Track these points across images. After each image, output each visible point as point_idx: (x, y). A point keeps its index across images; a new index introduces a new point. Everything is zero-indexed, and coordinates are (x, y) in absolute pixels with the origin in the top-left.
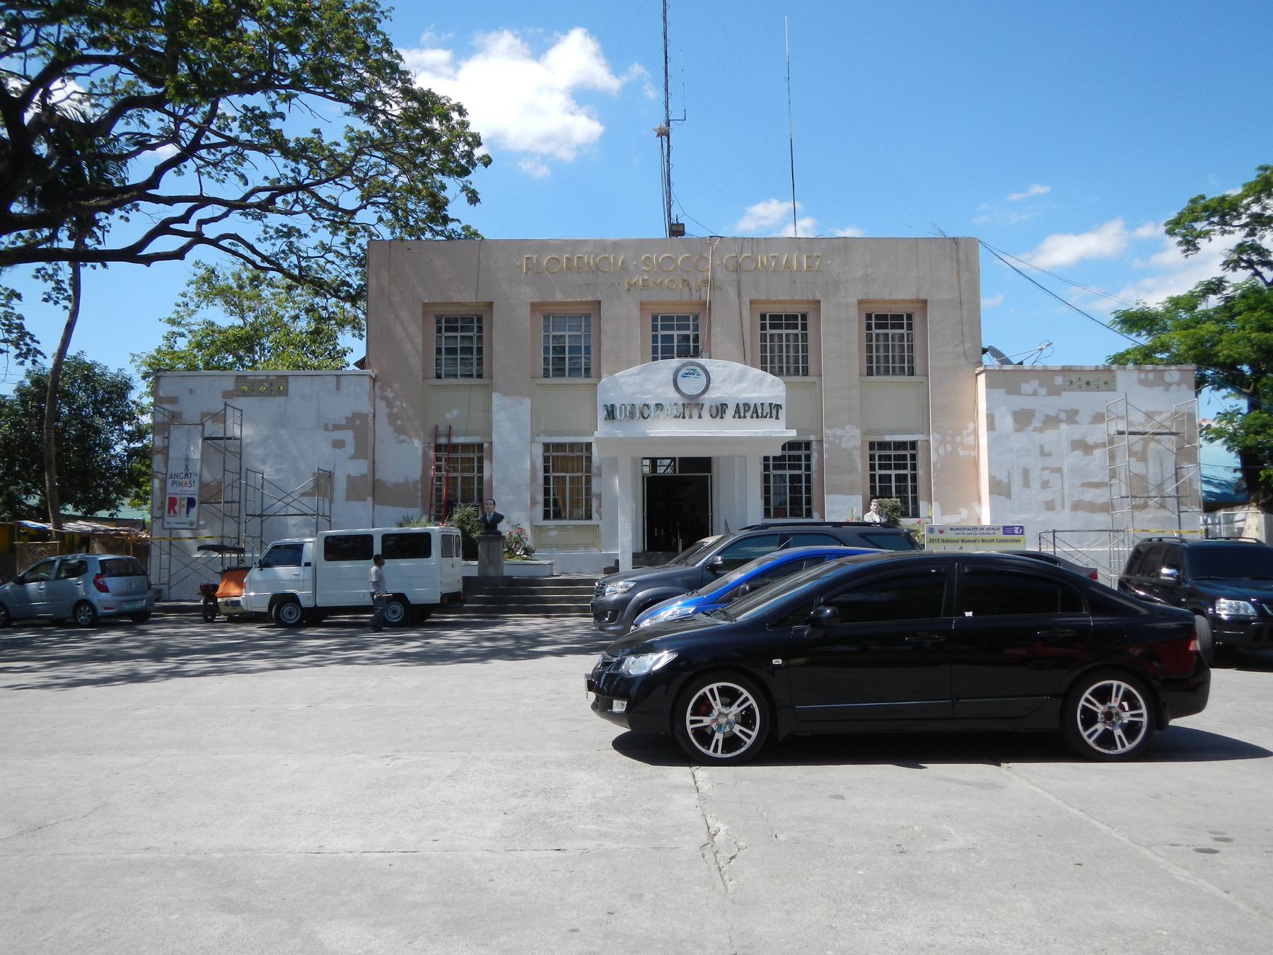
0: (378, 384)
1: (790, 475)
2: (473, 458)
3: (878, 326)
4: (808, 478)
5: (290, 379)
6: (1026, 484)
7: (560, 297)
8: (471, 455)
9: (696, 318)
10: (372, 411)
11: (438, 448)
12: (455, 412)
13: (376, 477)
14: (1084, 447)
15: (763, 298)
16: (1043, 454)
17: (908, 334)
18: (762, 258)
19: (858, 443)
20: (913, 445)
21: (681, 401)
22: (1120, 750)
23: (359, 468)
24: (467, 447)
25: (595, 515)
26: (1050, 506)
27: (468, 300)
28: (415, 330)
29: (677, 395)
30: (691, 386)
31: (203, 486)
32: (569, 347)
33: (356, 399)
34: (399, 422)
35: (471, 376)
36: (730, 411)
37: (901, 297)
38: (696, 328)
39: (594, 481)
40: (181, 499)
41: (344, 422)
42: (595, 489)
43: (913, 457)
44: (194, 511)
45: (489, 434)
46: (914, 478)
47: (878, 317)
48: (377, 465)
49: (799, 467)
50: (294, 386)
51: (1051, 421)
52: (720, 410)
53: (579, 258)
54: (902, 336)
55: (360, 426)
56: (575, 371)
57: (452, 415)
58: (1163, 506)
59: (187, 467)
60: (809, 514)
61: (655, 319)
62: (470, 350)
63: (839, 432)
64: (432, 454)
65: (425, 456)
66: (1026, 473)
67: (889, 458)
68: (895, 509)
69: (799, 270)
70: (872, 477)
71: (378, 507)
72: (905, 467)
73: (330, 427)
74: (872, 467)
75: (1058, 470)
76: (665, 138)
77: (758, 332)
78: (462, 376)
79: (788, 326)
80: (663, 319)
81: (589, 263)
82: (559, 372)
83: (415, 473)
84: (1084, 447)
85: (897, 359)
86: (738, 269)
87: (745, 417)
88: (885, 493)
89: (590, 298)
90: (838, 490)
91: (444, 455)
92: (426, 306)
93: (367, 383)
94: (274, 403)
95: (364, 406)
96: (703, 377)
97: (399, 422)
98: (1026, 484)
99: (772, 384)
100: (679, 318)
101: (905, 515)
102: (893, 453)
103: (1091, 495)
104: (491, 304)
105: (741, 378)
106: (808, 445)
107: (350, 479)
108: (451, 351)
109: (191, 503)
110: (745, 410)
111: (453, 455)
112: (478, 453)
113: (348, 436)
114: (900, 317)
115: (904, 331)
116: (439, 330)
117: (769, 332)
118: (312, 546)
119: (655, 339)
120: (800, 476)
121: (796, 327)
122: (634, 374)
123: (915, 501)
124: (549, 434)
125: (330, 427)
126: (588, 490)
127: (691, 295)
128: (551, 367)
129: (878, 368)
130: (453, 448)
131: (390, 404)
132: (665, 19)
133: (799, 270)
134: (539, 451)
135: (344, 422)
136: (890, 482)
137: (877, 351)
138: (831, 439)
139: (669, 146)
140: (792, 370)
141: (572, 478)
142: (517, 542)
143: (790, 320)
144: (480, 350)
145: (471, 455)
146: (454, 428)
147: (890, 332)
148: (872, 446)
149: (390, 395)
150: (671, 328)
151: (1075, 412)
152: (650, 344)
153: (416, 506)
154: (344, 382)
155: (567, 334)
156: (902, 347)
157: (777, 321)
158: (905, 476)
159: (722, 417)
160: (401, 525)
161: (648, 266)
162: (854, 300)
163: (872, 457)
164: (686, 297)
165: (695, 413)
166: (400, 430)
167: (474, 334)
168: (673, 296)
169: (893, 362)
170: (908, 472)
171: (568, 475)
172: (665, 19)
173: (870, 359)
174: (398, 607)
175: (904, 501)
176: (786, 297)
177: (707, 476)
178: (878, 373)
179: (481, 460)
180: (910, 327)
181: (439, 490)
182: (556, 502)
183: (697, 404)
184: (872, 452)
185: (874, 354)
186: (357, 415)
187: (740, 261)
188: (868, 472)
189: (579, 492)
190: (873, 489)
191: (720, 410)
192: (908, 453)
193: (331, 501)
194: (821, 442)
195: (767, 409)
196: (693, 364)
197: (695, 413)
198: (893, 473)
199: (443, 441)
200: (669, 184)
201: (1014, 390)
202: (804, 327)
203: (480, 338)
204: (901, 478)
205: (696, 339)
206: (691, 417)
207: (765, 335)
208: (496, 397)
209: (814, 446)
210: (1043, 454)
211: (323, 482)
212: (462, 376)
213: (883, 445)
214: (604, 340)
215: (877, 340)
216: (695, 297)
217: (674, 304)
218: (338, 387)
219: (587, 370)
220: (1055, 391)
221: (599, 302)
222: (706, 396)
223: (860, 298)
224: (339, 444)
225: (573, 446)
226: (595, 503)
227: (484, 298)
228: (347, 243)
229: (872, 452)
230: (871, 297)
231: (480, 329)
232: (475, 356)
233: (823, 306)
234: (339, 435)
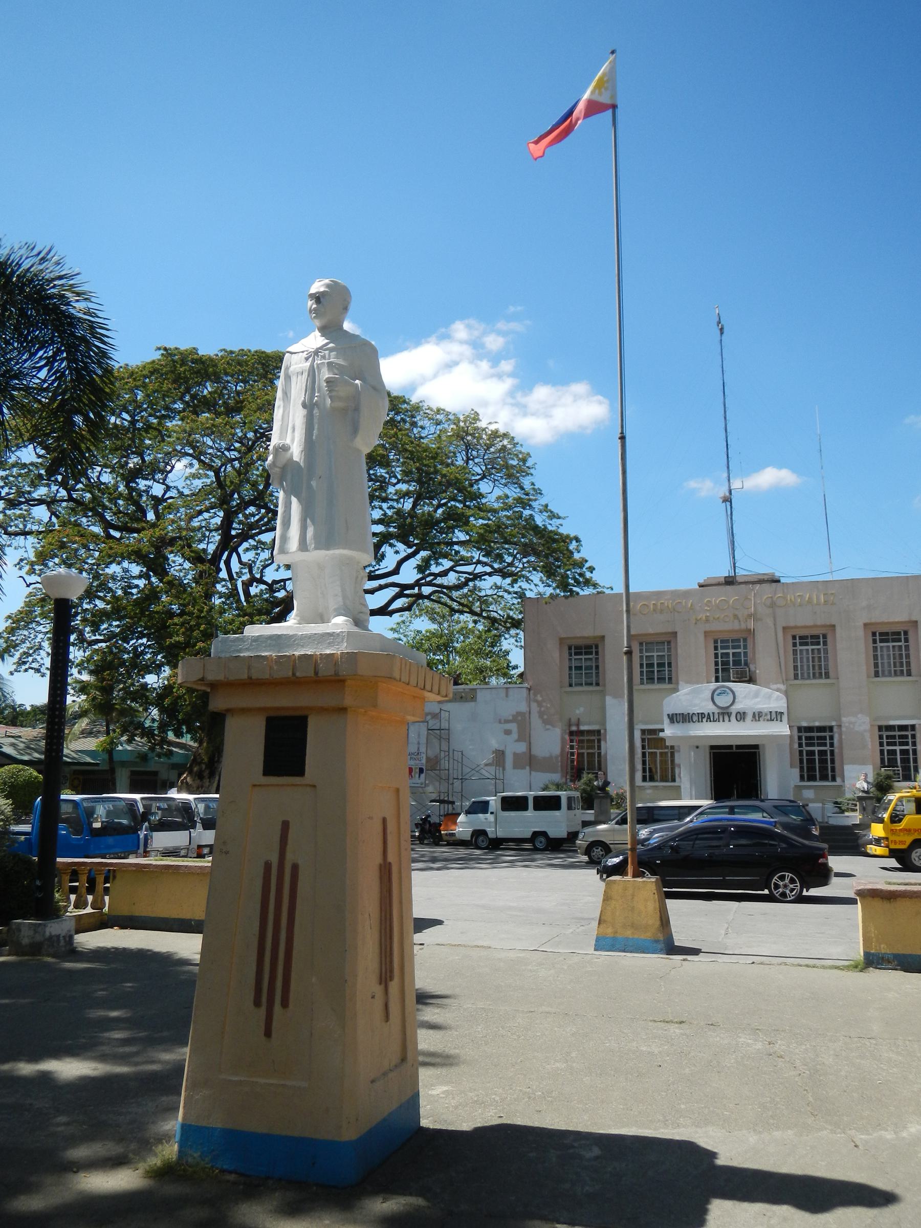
0: (532, 692)
1: (819, 751)
2: (594, 740)
3: (882, 641)
4: (832, 752)
5: (478, 691)
7: (651, 631)
8: (592, 738)
9: (745, 640)
10: (528, 710)
11: (571, 733)
12: (582, 709)
13: (532, 753)
15: (792, 624)
17: (905, 646)
19: (868, 727)
20: (913, 727)
21: (716, 711)
22: (789, 899)
23: (522, 748)
25: (677, 779)
27: (586, 635)
28: (556, 655)
29: (714, 707)
30: (723, 701)
31: (428, 760)
32: (657, 664)
33: (517, 702)
34: (545, 717)
35: (591, 684)
36: (749, 717)
37: (896, 620)
38: (745, 647)
39: (676, 755)
40: (416, 768)
41: (511, 718)
42: (677, 761)
43: (914, 736)
44: (423, 776)
45: (603, 722)
46: (915, 752)
47: (881, 634)
48: (532, 744)
49: (825, 745)
50: (480, 695)
52: (741, 716)
53: (661, 603)
54: (900, 647)
55: (522, 721)
56: (661, 680)
57: (579, 711)
59: (418, 748)
60: (834, 779)
61: (716, 642)
62: (589, 668)
63: (853, 719)
64: (567, 737)
65: (563, 739)
67: (894, 737)
68: (888, 777)
69: (818, 604)
70: (882, 752)
71: (532, 772)
72: (907, 744)
73: (502, 721)
74: (881, 744)
76: (728, 504)
77: (791, 648)
78: (587, 684)
79: (812, 644)
80: (722, 641)
81: (668, 606)
83: (557, 750)
85: (898, 664)
86: (773, 605)
87: (759, 720)
88: (892, 763)
89: (670, 630)
90: (854, 762)
91: (575, 738)
92: (562, 641)
93: (525, 691)
94: (469, 706)
95: (523, 708)
96: (731, 696)
97: (545, 717)
99: (778, 699)
100: (733, 641)
101: (907, 778)
102: (897, 733)
104: (603, 637)
105: (756, 695)
106: (831, 729)
107: (515, 755)
108: (579, 668)
109: (421, 771)
110: (758, 716)
111: (581, 738)
112: (597, 736)
113: (513, 727)
114: (899, 633)
115: (902, 643)
116: (570, 655)
117: (799, 648)
118: (494, 801)
119: (716, 656)
120: (826, 751)
121: (818, 644)
122: (688, 694)
123: (916, 770)
124: (646, 723)
125: (502, 721)
126: (673, 761)
127: (740, 625)
128: (645, 677)
129: (883, 671)
130: (581, 733)
131: (539, 704)
132: (725, 418)
133: (818, 604)
135: (511, 718)
136: (896, 755)
137: (882, 659)
138: (847, 724)
139: (731, 508)
140: (817, 675)
141: (661, 753)
142: (622, 799)
143: (815, 639)
144: (597, 667)
145: (592, 738)
146: (581, 720)
147: (891, 644)
148: (880, 728)
149: (539, 698)
150: (727, 648)
152: (713, 660)
153: (554, 772)
154: (511, 692)
155: (655, 654)
156: (901, 655)
157: (804, 640)
158: (908, 750)
159: (744, 721)
160: (544, 790)
161: (709, 606)
163: (881, 737)
164: (736, 626)
165: (726, 718)
166: (546, 722)
167: (593, 656)
168: (726, 626)
169: (895, 666)
170: (910, 747)
171: (658, 751)
172: (725, 418)
173: (876, 665)
174: (543, 839)
175: (906, 769)
176: (811, 623)
177: (755, 752)
178: (884, 675)
179: (599, 741)
180: (906, 640)
181: (572, 761)
182: (650, 769)
183: (728, 713)
184: (881, 733)
185: (880, 661)
186: (519, 714)
187: (775, 599)
188: (878, 748)
189: (666, 762)
190: (882, 760)
191: (741, 716)
192: (909, 733)
193: (504, 769)
194: (840, 726)
195: (774, 716)
196: (723, 687)
197: (726, 718)
198: (898, 748)
199: (574, 728)
200: (733, 535)
202: (825, 643)
203: (597, 659)
204: (904, 752)
205: (745, 653)
206: (724, 721)
207: (796, 650)
208: (609, 700)
209: (835, 729)
211: (500, 756)
212: (586, 684)
213: (890, 728)
214: (679, 659)
215: (882, 651)
216: (743, 626)
217: (729, 631)
218: (507, 696)
219: (670, 679)
221: (676, 633)
222: (733, 707)
223: (867, 621)
224: (508, 732)
227: (598, 633)
228: (512, 584)
229: (881, 733)
230: (873, 621)
231: (597, 653)
232: (594, 671)
233: (838, 629)
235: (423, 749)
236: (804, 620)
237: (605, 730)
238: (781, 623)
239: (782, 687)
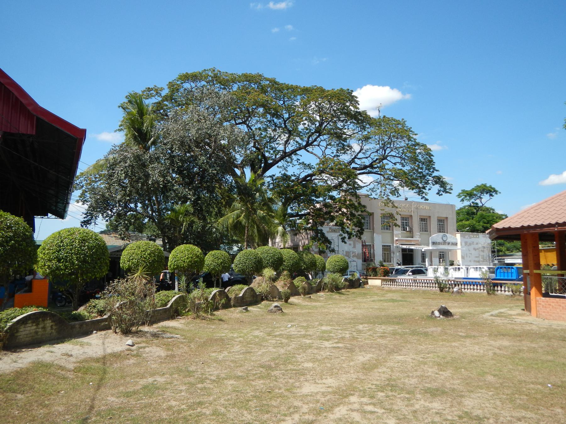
6: (467, 257)
11: (363, 245)
14: (475, 249)
16: (469, 251)
18: (421, 207)
26: (470, 261)
30: (445, 239)
36: (450, 244)
51: (470, 244)
52: (449, 244)
58: (486, 261)
66: (467, 254)
75: (471, 254)
84: (475, 249)
86: (417, 208)
98: (467, 257)
105: (451, 237)
124: (383, 243)
130: (366, 245)
151: (473, 242)
162: (436, 216)
191: (449, 244)
201: (464, 238)
210: (469, 251)
216: (410, 214)
220: (470, 238)
225: (387, 246)
226: (392, 259)
236: (424, 214)
237: (373, 245)
238: (419, 214)
239: (419, 234)
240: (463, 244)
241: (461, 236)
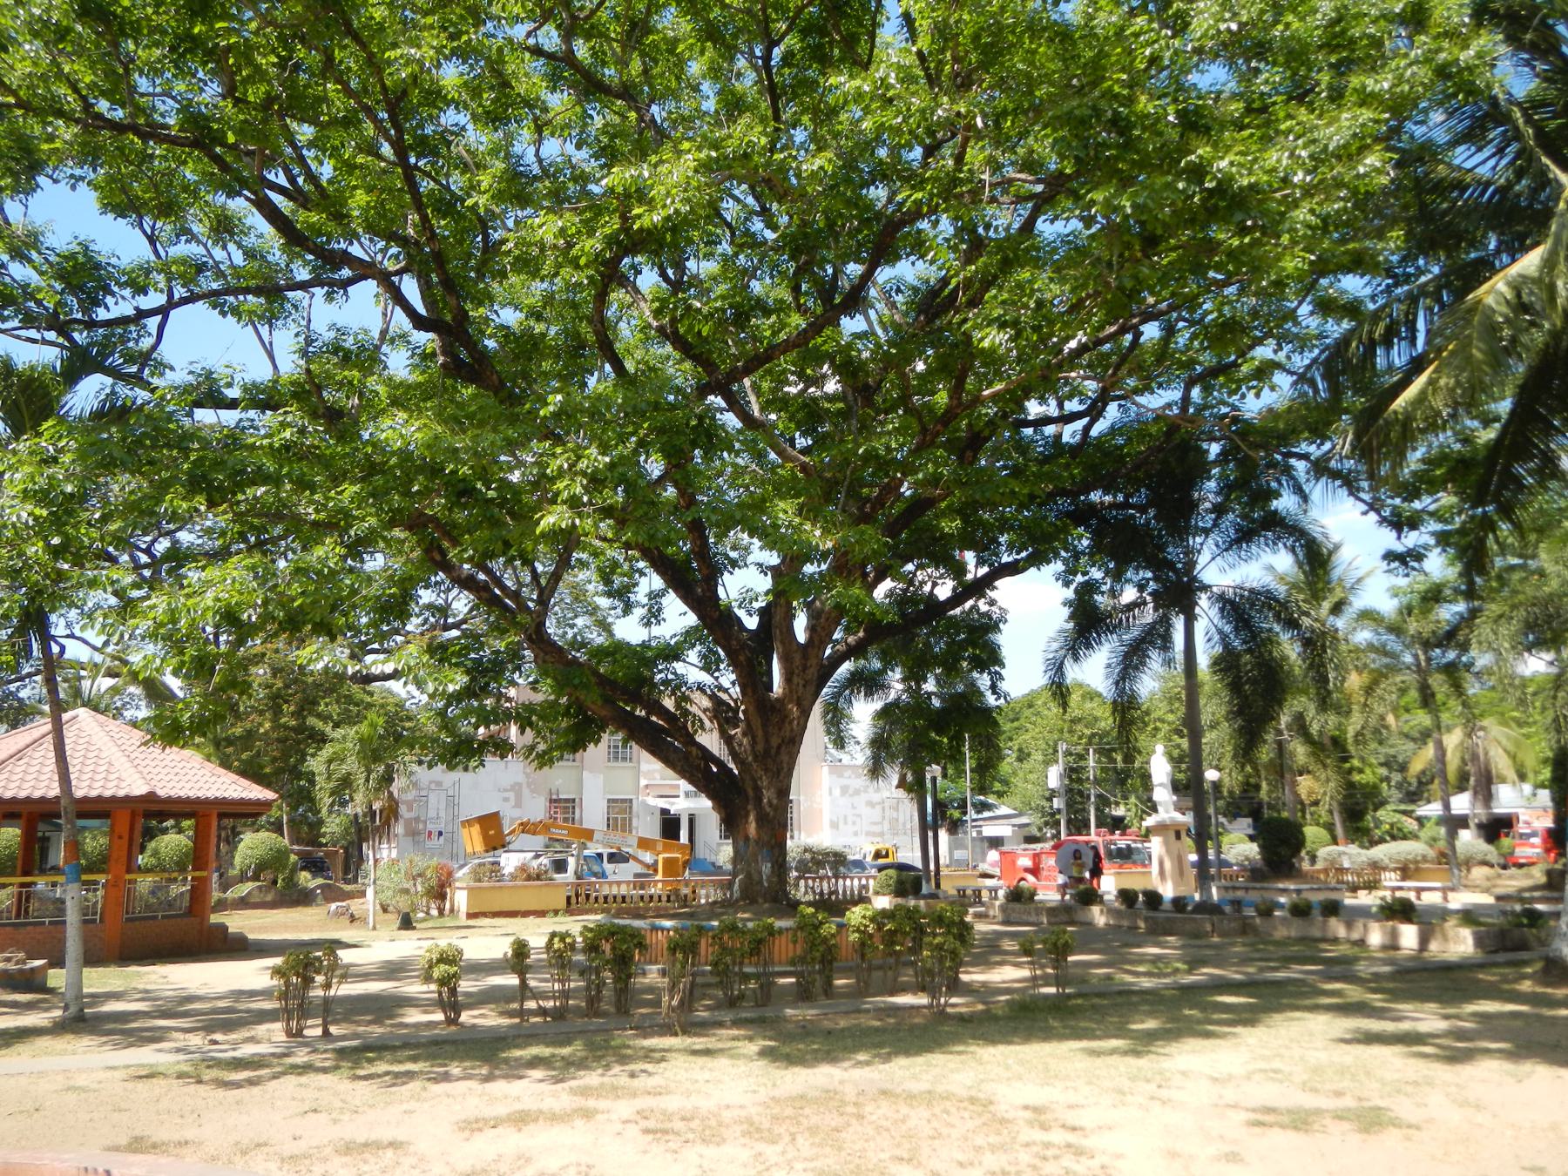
11: (551, 801)
14: (871, 804)
16: (854, 807)
24: (567, 800)
26: (856, 834)
55: (516, 788)
56: (624, 759)
75: (859, 816)
82: (616, 758)
84: (871, 804)
103: (877, 829)
109: (440, 834)
113: (511, 795)
134: (605, 804)
166: (533, 791)
201: (841, 776)
210: (854, 807)
224: (506, 800)
234: (506, 794)
235: (442, 814)
240: (837, 792)
241: (831, 773)
